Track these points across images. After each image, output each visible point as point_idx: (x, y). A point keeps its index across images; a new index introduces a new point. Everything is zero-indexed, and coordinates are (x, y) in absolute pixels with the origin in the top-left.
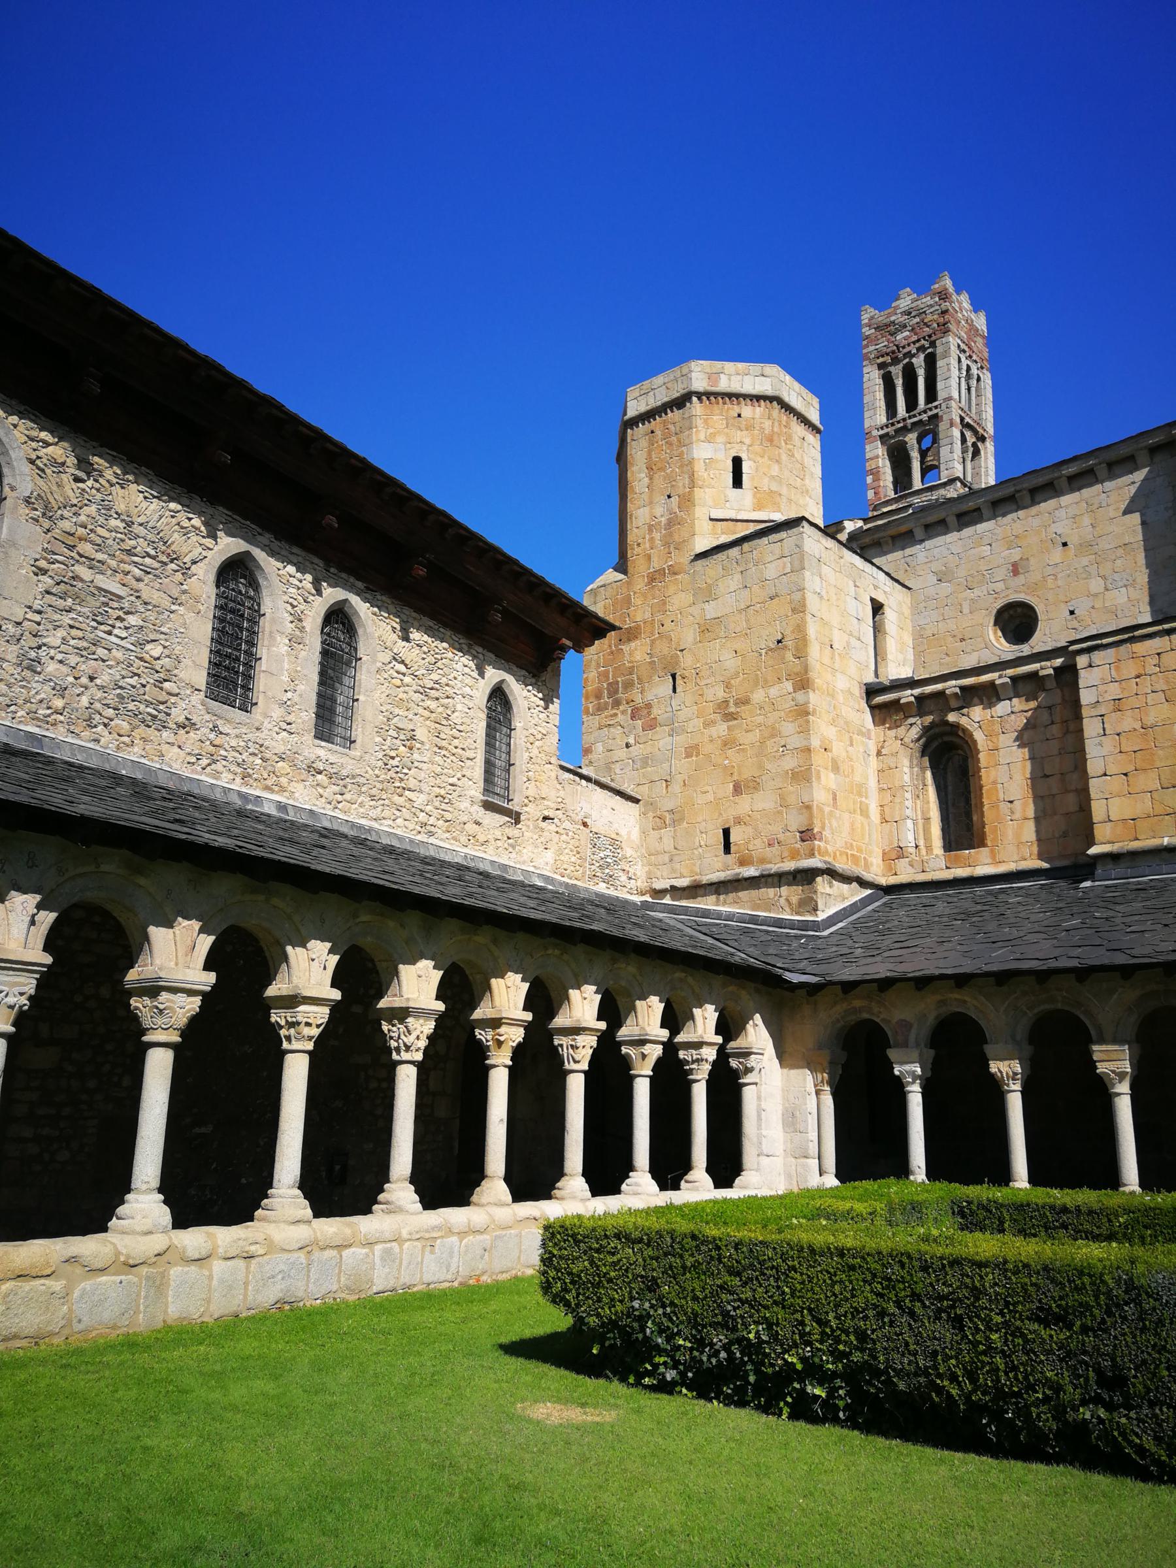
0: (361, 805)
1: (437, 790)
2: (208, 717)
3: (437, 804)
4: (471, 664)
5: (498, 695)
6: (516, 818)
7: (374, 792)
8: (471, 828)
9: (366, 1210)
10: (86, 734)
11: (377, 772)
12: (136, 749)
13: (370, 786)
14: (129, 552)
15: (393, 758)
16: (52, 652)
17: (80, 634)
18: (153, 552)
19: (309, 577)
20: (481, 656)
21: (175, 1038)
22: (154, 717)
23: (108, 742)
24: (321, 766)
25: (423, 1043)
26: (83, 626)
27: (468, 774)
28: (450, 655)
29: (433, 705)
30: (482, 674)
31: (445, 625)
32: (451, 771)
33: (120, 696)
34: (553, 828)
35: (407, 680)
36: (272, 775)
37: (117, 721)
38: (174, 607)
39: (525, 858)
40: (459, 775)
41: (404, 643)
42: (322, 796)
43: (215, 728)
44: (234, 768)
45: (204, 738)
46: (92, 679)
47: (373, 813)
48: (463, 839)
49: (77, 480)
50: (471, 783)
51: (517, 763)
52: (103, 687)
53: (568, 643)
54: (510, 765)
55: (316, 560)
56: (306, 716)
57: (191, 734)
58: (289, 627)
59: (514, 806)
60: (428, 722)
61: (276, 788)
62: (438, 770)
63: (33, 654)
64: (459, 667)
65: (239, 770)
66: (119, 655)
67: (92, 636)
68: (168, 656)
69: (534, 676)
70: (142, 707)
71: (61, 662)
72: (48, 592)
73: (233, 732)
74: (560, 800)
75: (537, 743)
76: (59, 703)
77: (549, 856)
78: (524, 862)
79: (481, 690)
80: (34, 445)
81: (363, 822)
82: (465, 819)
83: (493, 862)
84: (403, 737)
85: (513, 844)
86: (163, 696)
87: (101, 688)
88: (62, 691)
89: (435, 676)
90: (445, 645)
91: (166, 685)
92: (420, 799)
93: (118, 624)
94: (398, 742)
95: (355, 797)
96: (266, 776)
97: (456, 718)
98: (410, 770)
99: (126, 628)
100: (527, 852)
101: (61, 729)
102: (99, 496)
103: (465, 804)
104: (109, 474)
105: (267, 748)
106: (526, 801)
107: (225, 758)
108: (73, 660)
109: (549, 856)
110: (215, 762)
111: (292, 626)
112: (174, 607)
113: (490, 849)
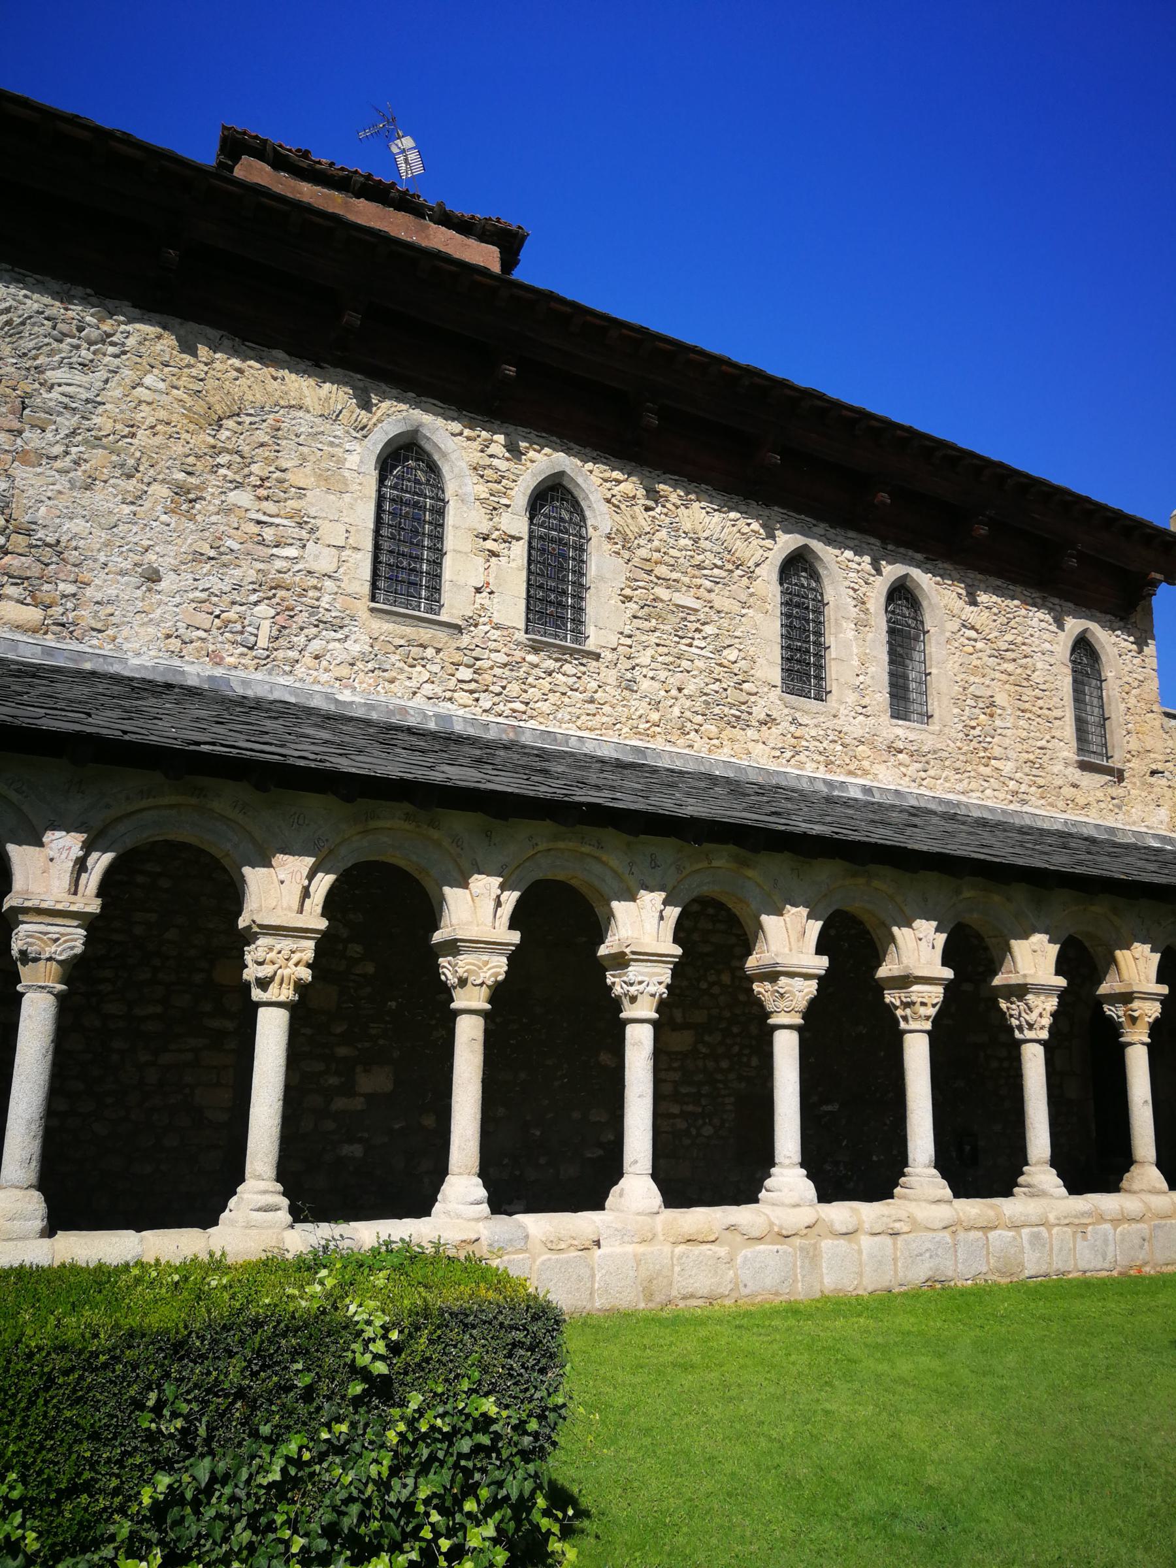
0: (947, 779)
1: (1026, 756)
2: (786, 711)
3: (1027, 770)
4: (1048, 618)
5: (1083, 647)
6: (1119, 776)
7: (958, 765)
8: (1068, 791)
9: (1007, 1193)
10: (681, 742)
11: (959, 744)
12: (725, 750)
14: (699, 567)
15: (973, 728)
16: (645, 671)
17: (665, 650)
18: (719, 563)
19: (867, 559)
20: (1058, 608)
21: (798, 1021)
22: (738, 718)
23: (701, 747)
24: (901, 745)
25: (1047, 1021)
26: (667, 643)
27: (1058, 734)
28: (1023, 612)
29: (1010, 667)
30: (1061, 627)
31: (1015, 582)
32: (1038, 734)
33: (707, 703)
34: (1164, 782)
35: (979, 645)
37: (706, 726)
38: (744, 611)
39: (1135, 818)
40: (1048, 737)
41: (972, 608)
43: (794, 721)
44: (816, 757)
46: (680, 690)
47: (960, 787)
48: (1061, 804)
49: (648, 509)
50: (1062, 744)
51: (1113, 716)
52: (691, 696)
53: (1158, 576)
54: (1105, 719)
55: (872, 540)
56: (881, 697)
57: (773, 729)
58: (854, 612)
59: (1115, 763)
60: (1007, 686)
61: (859, 772)
62: (1024, 734)
63: (629, 675)
64: (1035, 622)
65: (822, 758)
66: (700, 664)
67: (676, 650)
68: (744, 659)
69: (1122, 619)
70: (726, 710)
71: (652, 678)
72: (635, 617)
73: (811, 722)
74: (1168, 751)
75: (1134, 692)
76: (655, 716)
77: (1163, 813)
78: (1134, 823)
79: (1062, 644)
80: (608, 485)
81: (951, 796)
82: (1060, 782)
83: (1097, 826)
84: (981, 705)
85: (1119, 804)
86: (743, 697)
87: (689, 697)
88: (656, 705)
89: (1009, 637)
90: (1016, 602)
91: (745, 686)
92: (1008, 767)
93: (697, 635)
94: (977, 711)
96: (848, 761)
97: (1037, 677)
98: (993, 738)
99: (704, 638)
100: (1136, 812)
101: (659, 739)
102: (668, 520)
103: (1058, 767)
104: (673, 498)
106: (1128, 756)
108: (662, 675)
109: (1163, 813)
110: (798, 753)
111: (856, 610)
112: (744, 611)
113: (1093, 812)
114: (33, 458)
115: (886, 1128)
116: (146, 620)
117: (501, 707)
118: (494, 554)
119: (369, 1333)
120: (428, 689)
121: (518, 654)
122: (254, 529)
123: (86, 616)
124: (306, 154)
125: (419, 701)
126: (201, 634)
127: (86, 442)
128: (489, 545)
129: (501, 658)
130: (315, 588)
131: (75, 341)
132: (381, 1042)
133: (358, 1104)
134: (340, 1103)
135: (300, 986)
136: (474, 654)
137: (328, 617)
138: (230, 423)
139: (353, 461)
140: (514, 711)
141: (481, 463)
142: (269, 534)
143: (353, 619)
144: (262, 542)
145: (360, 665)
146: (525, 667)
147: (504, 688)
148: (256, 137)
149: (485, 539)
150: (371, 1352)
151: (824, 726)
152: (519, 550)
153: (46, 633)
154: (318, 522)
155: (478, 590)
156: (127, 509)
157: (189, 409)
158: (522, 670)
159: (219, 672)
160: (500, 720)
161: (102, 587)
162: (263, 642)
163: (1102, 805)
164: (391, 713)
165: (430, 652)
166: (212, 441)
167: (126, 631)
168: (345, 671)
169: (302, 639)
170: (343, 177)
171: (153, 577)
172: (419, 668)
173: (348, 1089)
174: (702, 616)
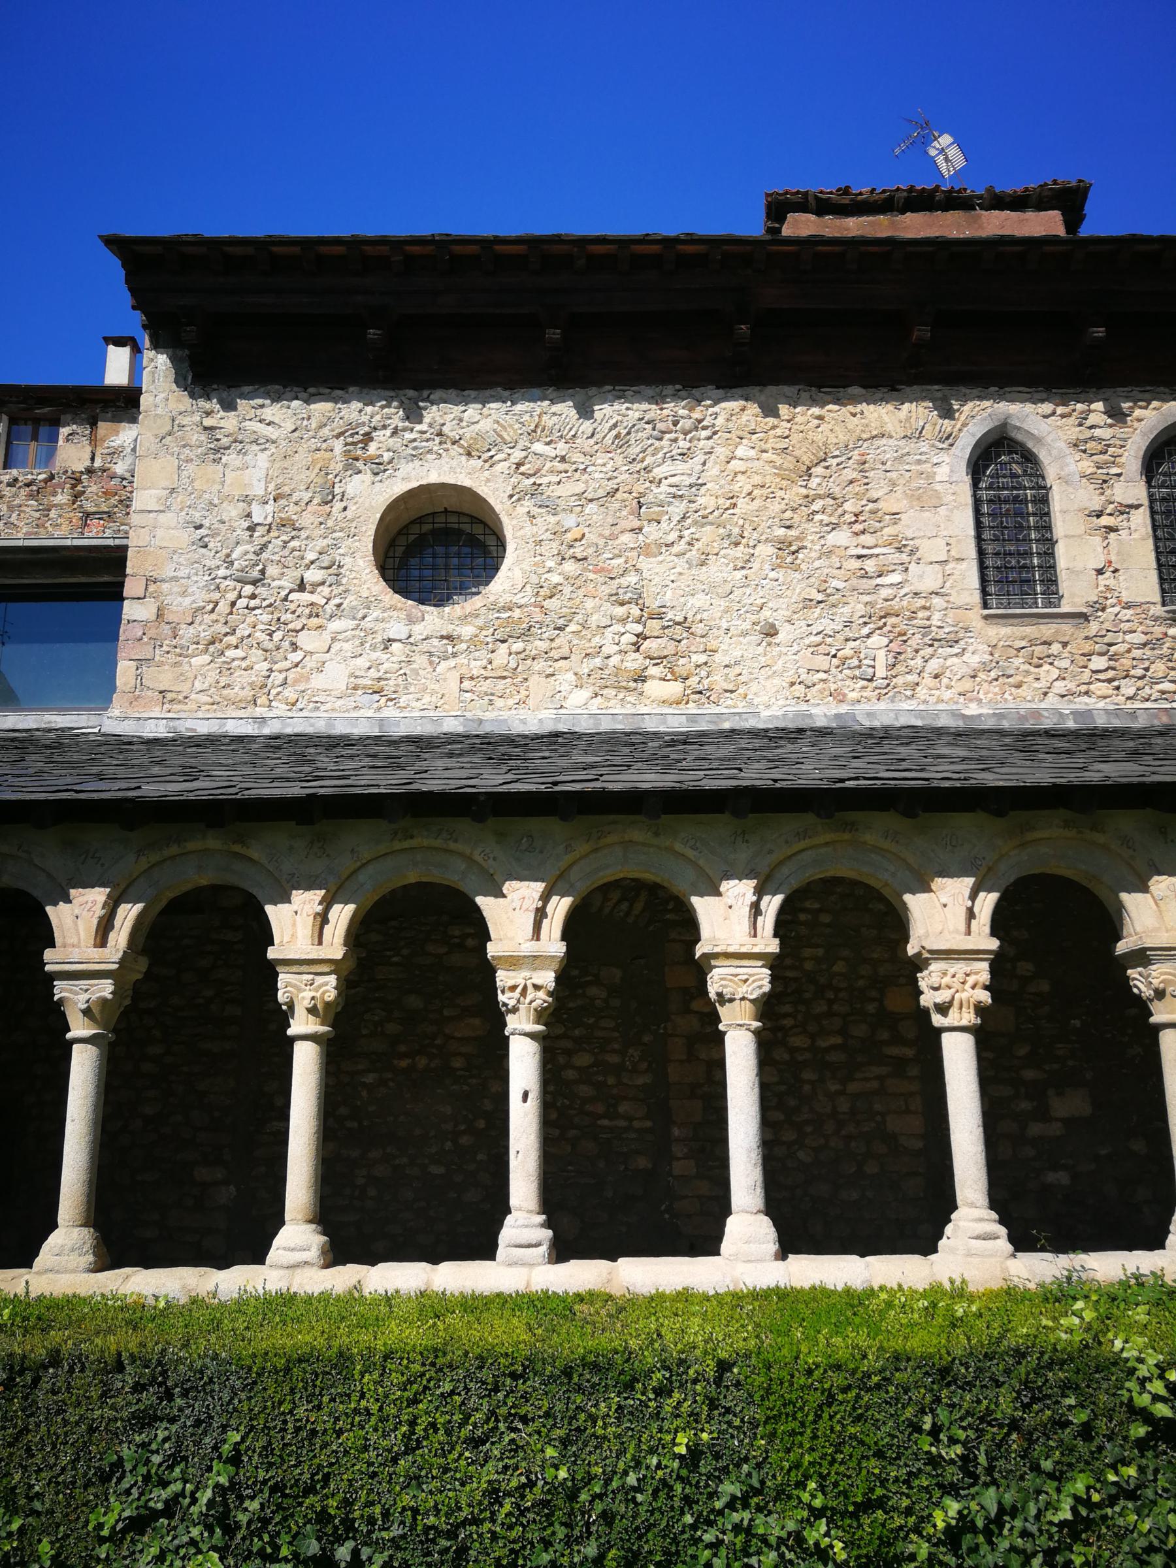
114: (654, 549)
116: (770, 673)
117: (1147, 690)
118: (1111, 529)
119: (1143, 1371)
120: (1060, 687)
121: (1158, 630)
122: (857, 564)
123: (718, 680)
124: (846, 191)
125: (1052, 701)
126: (822, 675)
127: (695, 523)
128: (1105, 521)
129: (1139, 638)
130: (924, 608)
131: (673, 436)
132: (1070, 1063)
133: (1056, 1129)
134: (1035, 1129)
135: (980, 1009)
136: (1106, 640)
137: (941, 634)
138: (818, 470)
139: (942, 473)
140: (1163, 692)
141: (1082, 437)
142: (870, 566)
143: (967, 630)
144: (865, 576)
145: (982, 676)
147: (1147, 669)
148: (798, 192)
149: (1098, 516)
150: (1150, 1393)
152: (1141, 520)
153: (687, 703)
154: (917, 542)
155: (1100, 572)
156: (739, 574)
157: (780, 468)
159: (843, 709)
160: (1148, 705)
161: (729, 650)
162: (881, 672)
164: (1023, 718)
165: (1056, 648)
166: (804, 491)
167: (754, 687)
168: (967, 684)
169: (919, 661)
170: (886, 199)
171: (771, 632)
172: (1046, 667)
173: (1043, 1114)
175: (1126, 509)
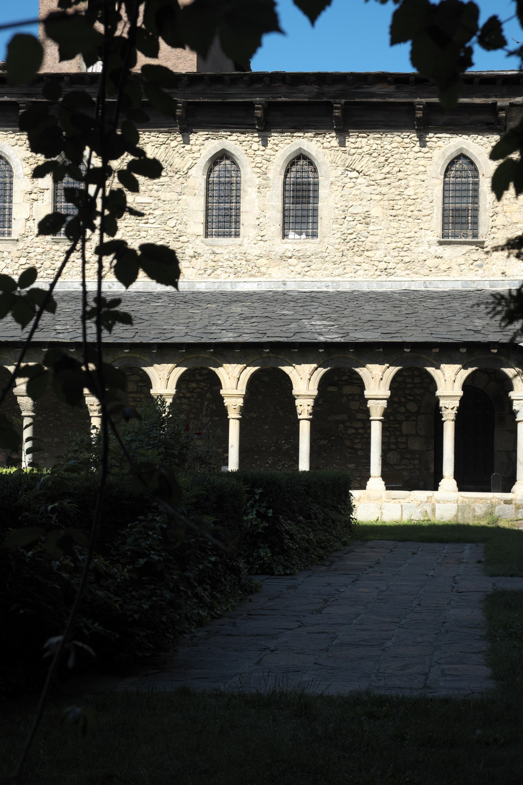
0: (325, 269)
2: (207, 248)
13: (331, 256)
15: (351, 234)
17: (131, 229)
29: (384, 190)
36: (254, 268)
38: (180, 197)
42: (292, 271)
45: (206, 259)
47: (336, 272)
61: (259, 274)
67: (137, 227)
68: (180, 224)
78: (494, 275)
91: (181, 239)
92: (378, 255)
95: (320, 265)
96: (250, 269)
105: (249, 254)
107: (222, 267)
110: (215, 270)
111: (260, 179)
112: (180, 197)
115: (267, 465)
128: (33, 196)
129: (41, 250)
136: (27, 251)
146: (53, 252)
149: (30, 194)
151: (233, 252)
158: (51, 254)
163: (463, 267)
174: (153, 206)
175: (42, 191)
